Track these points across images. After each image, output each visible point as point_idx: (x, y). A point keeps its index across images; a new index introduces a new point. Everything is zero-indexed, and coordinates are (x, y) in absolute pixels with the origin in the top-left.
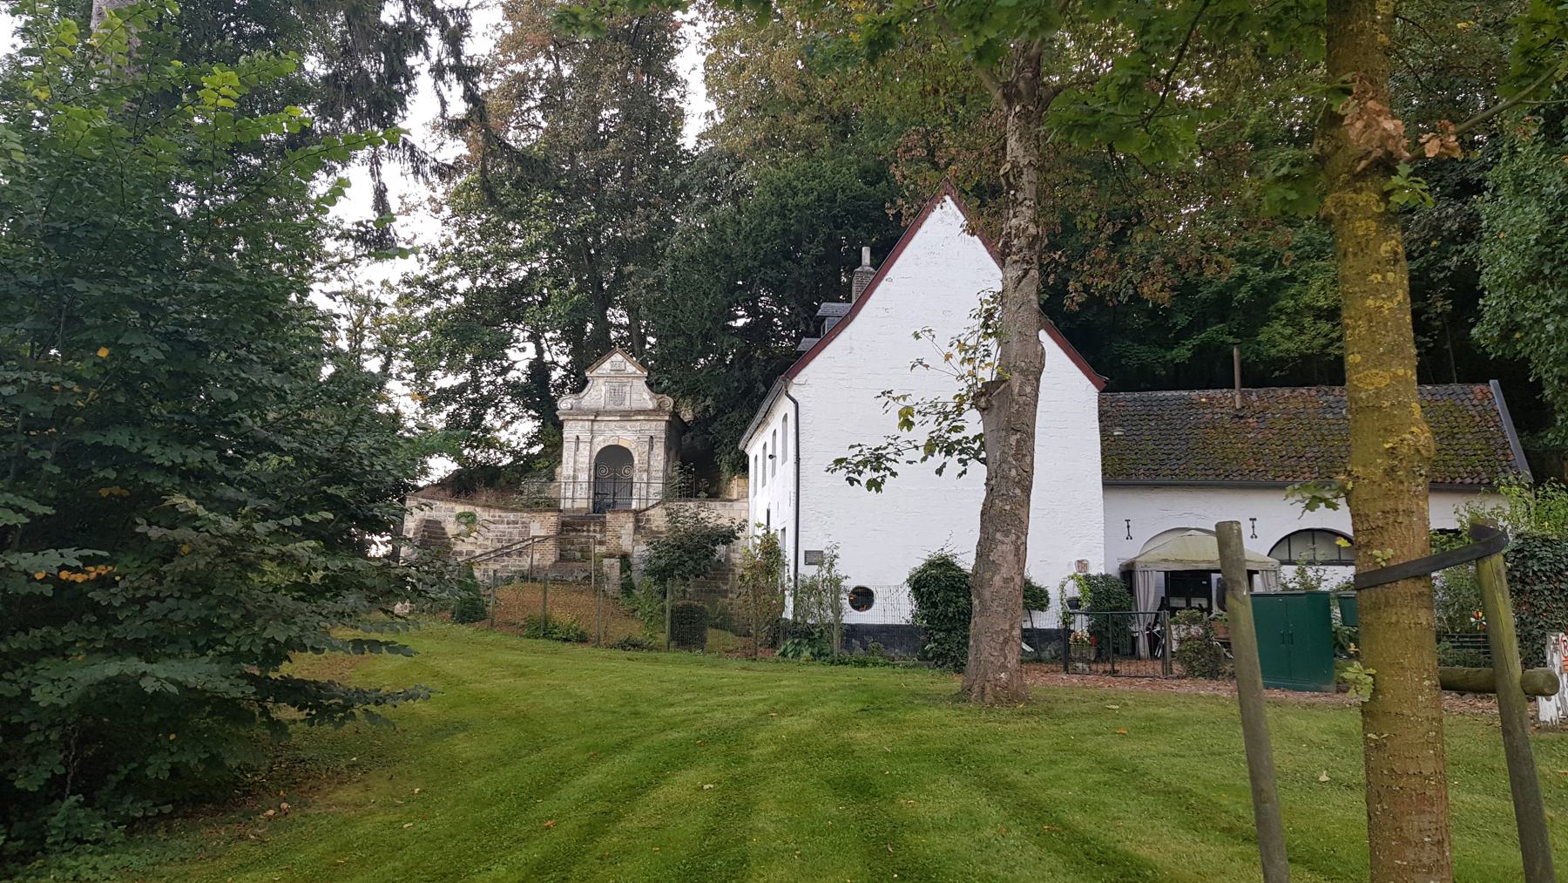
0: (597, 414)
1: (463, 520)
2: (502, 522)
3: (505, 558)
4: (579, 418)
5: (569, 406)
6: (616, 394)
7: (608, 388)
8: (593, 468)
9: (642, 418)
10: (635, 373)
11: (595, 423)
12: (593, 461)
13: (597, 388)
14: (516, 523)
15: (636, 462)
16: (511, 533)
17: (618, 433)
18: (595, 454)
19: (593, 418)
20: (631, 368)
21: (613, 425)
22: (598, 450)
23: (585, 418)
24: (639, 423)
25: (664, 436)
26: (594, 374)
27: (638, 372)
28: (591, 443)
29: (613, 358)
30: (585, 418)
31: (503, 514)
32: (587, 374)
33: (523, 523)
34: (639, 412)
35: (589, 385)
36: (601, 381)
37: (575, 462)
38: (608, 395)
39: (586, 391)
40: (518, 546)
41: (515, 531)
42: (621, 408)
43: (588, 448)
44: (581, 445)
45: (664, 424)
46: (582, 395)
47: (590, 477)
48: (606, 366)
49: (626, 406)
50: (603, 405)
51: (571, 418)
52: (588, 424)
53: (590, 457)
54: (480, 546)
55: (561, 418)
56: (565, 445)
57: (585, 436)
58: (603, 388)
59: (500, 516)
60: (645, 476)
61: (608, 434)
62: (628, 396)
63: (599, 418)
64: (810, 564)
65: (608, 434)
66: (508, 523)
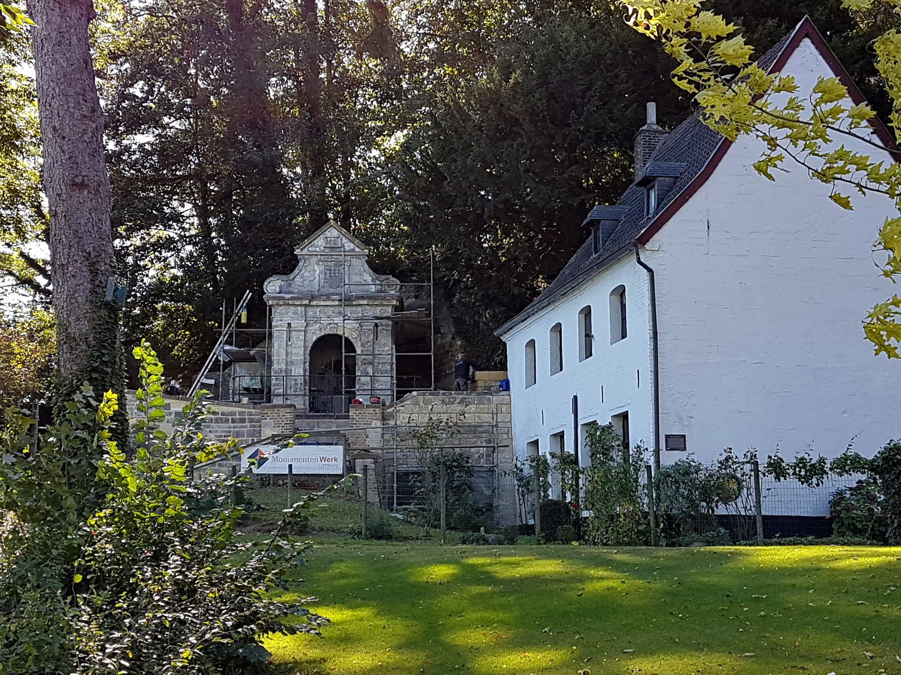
2: (227, 421)
6: (334, 276)
7: (322, 268)
9: (365, 302)
10: (353, 250)
11: (308, 309)
12: (308, 352)
13: (309, 268)
18: (310, 345)
19: (307, 302)
21: (330, 311)
22: (315, 338)
23: (298, 303)
24: (360, 309)
26: (305, 251)
27: (357, 249)
28: (305, 331)
29: (328, 234)
30: (298, 303)
35: (301, 264)
36: (314, 259)
38: (322, 276)
39: (296, 271)
43: (302, 337)
46: (292, 276)
47: (305, 371)
48: (319, 243)
53: (305, 347)
57: (298, 324)
58: (316, 267)
60: (370, 370)
63: (314, 303)
64: (685, 447)
66: (233, 421)
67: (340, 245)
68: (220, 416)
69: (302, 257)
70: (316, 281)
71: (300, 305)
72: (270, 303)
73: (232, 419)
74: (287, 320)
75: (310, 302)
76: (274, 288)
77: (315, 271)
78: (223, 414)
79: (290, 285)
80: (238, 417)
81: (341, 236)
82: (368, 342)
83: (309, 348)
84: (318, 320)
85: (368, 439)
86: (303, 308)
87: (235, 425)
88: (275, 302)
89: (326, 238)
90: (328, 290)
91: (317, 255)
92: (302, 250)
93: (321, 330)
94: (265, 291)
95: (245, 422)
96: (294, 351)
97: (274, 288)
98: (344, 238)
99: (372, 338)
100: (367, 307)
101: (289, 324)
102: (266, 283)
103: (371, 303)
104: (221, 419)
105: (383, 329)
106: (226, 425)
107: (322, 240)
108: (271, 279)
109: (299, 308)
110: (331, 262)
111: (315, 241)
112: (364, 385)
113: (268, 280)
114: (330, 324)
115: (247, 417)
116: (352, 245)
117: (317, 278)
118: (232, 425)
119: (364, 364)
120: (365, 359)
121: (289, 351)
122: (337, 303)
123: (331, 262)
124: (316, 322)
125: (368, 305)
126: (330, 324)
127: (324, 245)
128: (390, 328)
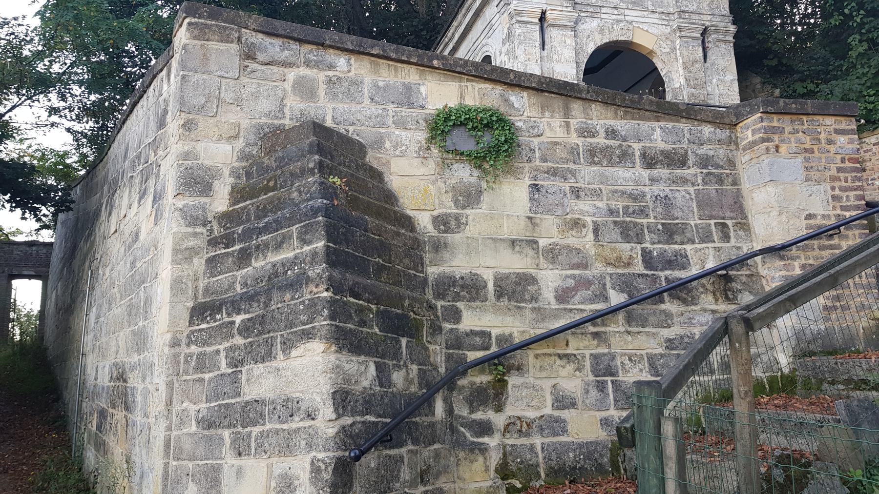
1: (462, 140)
2: (625, 157)
3: (670, 306)
14: (675, 160)
16: (666, 202)
22: (591, 48)
28: (574, 29)
31: (624, 125)
33: (704, 162)
43: (570, 41)
44: (551, 33)
54: (553, 254)
59: (611, 133)
66: (649, 161)
68: (601, 140)
73: (644, 155)
80: (661, 145)
93: (601, 31)
95: (683, 163)
101: (544, 13)
105: (719, 40)
114: (619, 21)
118: (645, 173)
120: (693, 95)
124: (593, 15)
126: (619, 21)
128: (731, 39)
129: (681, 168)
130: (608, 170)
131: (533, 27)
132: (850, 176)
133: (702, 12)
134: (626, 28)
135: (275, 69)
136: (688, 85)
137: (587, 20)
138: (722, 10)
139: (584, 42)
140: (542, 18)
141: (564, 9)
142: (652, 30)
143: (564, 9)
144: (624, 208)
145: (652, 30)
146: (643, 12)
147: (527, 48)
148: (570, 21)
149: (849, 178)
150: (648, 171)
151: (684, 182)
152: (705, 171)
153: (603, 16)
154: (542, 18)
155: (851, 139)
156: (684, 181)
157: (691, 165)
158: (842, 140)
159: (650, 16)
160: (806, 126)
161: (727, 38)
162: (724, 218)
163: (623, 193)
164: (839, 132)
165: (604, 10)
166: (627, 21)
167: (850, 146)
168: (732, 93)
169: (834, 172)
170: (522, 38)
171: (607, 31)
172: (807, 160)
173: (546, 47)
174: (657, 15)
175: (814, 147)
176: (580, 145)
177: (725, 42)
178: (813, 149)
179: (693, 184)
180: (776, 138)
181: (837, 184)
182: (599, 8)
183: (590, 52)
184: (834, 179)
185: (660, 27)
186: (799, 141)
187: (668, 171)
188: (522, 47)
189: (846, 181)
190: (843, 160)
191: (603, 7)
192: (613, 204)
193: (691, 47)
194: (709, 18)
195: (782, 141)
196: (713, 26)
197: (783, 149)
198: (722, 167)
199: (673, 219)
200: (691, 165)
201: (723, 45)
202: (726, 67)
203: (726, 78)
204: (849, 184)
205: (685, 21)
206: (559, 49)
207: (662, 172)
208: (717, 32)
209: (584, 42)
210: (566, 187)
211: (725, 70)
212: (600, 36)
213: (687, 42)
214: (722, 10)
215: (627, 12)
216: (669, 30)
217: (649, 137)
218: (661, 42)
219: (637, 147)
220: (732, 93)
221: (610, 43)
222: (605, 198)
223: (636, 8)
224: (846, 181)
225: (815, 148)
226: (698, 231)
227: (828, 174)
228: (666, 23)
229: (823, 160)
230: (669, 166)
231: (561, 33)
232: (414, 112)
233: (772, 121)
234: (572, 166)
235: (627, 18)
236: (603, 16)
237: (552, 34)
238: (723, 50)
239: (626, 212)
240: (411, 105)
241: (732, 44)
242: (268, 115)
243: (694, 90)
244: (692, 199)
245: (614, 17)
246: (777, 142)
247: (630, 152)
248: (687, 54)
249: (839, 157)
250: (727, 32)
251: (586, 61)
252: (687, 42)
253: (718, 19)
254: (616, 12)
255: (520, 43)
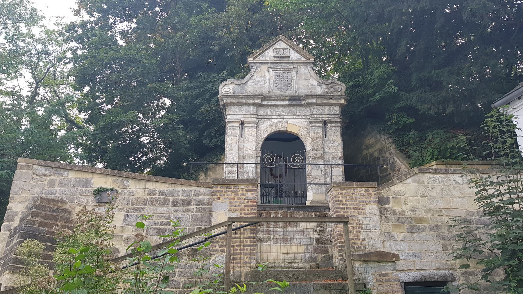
0: (264, 98)
2: (165, 203)
4: (244, 101)
5: (231, 91)
8: (260, 155)
9: (314, 101)
13: (260, 74)
14: (187, 203)
15: (308, 147)
17: (287, 118)
18: (261, 141)
19: (258, 101)
20: (295, 56)
21: (280, 111)
22: (266, 135)
23: (251, 101)
25: (339, 120)
26: (257, 60)
27: (303, 59)
28: (256, 127)
29: (277, 46)
30: (251, 101)
32: (250, 60)
34: (312, 96)
35: (253, 70)
36: (265, 67)
37: (239, 149)
38: (272, 81)
39: (249, 76)
40: (191, 241)
41: (186, 217)
42: (288, 93)
43: (254, 133)
45: (337, 110)
46: (244, 81)
48: (269, 54)
49: (293, 91)
50: (267, 90)
51: (235, 101)
52: (252, 109)
53: (257, 143)
55: (221, 103)
56: (228, 130)
57: (250, 120)
58: (267, 74)
61: (275, 119)
62: (294, 82)
63: (266, 103)
65: (275, 119)
67: (288, 55)
68: (157, 196)
69: (253, 64)
70: (267, 84)
71: (253, 104)
72: (225, 101)
73: (173, 201)
74: (240, 117)
75: (261, 101)
76: (227, 90)
77: (265, 76)
78: (162, 193)
79: (243, 88)
80: (181, 197)
81: (289, 47)
82: (319, 138)
83: (261, 144)
84: (268, 118)
85: (361, 231)
86: (256, 108)
87: (176, 208)
88: (229, 101)
89: (276, 49)
90: (276, 92)
91: (267, 63)
92: (254, 59)
94: (220, 92)
95: (189, 204)
96: (247, 145)
97: (228, 90)
98: (291, 50)
99: (321, 134)
100: (315, 107)
102: (221, 86)
103: (319, 101)
104: (159, 200)
106: (164, 209)
107: (272, 50)
108: (226, 82)
109: (252, 107)
110: (280, 68)
111: (266, 52)
112: (316, 178)
113: (223, 83)
114: (280, 122)
115: (193, 197)
116: (299, 55)
117: (268, 82)
118: (173, 208)
119: (316, 158)
120: (315, 154)
121: (242, 146)
122: (287, 102)
123: (280, 68)
125: (317, 104)
126: (280, 122)
127: (274, 55)
128: (339, 125)
129: (188, 206)
130: (158, 208)
131: (236, 128)
132: (250, 209)
133: (322, 113)
134: (284, 124)
135: (43, 177)
136: (313, 149)
137: (265, 122)
138: (335, 111)
139: (262, 132)
140: (242, 123)
141: (252, 119)
142: (298, 124)
143: (252, 119)
144: (160, 222)
145: (298, 124)
146: (293, 117)
147: (232, 138)
148: (254, 124)
149: (249, 210)
150: (174, 207)
151: (188, 211)
152: (198, 207)
153: (273, 120)
154: (242, 123)
155: (253, 193)
156: (188, 211)
157: (192, 205)
158: (249, 194)
159: (297, 118)
160: (233, 189)
161: (337, 125)
162: (201, 226)
163: (162, 216)
164: (247, 190)
165: (273, 117)
166: (285, 121)
167: (252, 196)
168: (337, 152)
169: (242, 207)
170: (230, 133)
171: (274, 127)
172: (231, 203)
173: (243, 136)
174: (300, 117)
175: (235, 197)
176: (148, 198)
177: (335, 127)
178: (235, 198)
179: (192, 212)
180: (218, 194)
181: (243, 212)
182: (270, 117)
183: (265, 137)
184: (241, 210)
185: (302, 122)
186: (229, 195)
187: (183, 207)
188: (230, 137)
189: (248, 210)
190: (248, 202)
191: (273, 116)
192: (157, 221)
193: (316, 131)
194: (327, 116)
195: (221, 195)
196: (328, 120)
197: (221, 198)
198: (206, 205)
199: (180, 226)
200: (192, 205)
201: (334, 129)
202: (334, 139)
203: (334, 145)
204: (249, 212)
205: (314, 119)
206: (248, 137)
207: (181, 208)
208: (331, 122)
209: (262, 132)
210: (139, 214)
211: (334, 141)
212: (271, 129)
213: (314, 129)
214: (335, 111)
215: (285, 117)
216: (307, 123)
217: (177, 194)
218: (302, 130)
219: (171, 198)
220: (337, 152)
221: (275, 132)
222: (154, 218)
223: (290, 115)
224: (248, 210)
225: (236, 198)
226: (189, 231)
227: (239, 208)
228: (305, 120)
229: (239, 202)
230: (183, 205)
231: (250, 129)
232: (87, 189)
233: (217, 187)
234: (143, 207)
235: (285, 120)
236: (273, 120)
237: (246, 130)
238: (334, 131)
239: (161, 224)
240: (87, 187)
241: (339, 128)
242: (37, 193)
243: (316, 151)
244: (190, 218)
245: (278, 120)
246: (218, 196)
247: (168, 200)
248: (314, 134)
249: (246, 201)
250: (336, 122)
251: (262, 141)
252: (314, 129)
253: (332, 116)
254: (279, 117)
255: (229, 136)
